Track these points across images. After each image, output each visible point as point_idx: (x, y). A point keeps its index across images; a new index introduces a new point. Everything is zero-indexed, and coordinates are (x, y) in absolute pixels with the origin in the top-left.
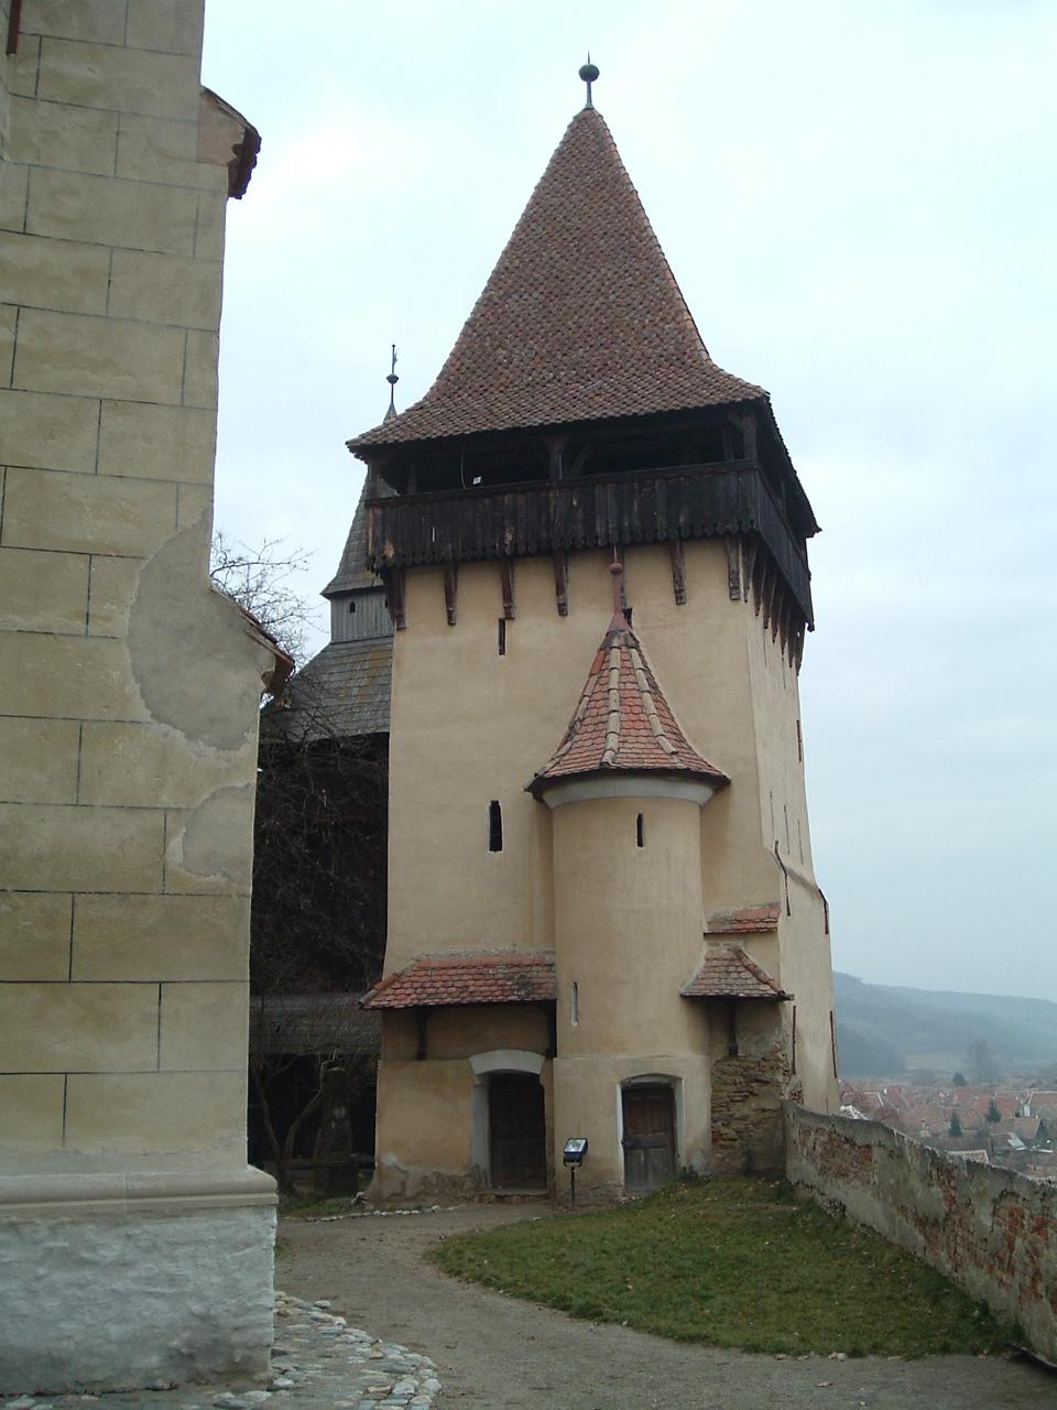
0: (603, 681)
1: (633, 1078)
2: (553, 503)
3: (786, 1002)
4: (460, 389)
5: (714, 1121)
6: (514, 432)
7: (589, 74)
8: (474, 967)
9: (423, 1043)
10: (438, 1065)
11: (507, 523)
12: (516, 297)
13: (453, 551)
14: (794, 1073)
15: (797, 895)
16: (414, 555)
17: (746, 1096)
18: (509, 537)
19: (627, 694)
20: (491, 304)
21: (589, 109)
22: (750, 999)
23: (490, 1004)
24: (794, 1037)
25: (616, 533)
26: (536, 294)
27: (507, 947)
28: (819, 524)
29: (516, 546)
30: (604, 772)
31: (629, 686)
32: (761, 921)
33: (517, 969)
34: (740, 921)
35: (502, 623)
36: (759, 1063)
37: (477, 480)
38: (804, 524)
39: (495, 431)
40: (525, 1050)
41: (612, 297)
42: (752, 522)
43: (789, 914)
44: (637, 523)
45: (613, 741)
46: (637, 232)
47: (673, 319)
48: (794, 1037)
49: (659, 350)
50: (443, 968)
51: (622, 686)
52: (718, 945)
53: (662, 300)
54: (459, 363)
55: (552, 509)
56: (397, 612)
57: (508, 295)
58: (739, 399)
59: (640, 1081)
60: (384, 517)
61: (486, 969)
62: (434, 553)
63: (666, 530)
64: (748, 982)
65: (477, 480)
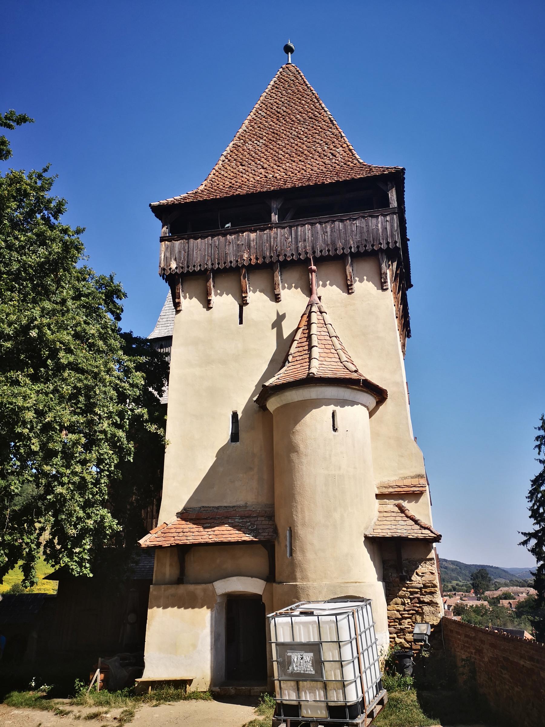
17: (413, 614)
18: (246, 256)
19: (322, 338)
22: (417, 539)
29: (250, 260)
31: (323, 333)
34: (399, 486)
36: (421, 589)
40: (252, 577)
45: (315, 363)
50: (198, 519)
51: (319, 333)
55: (272, 240)
56: (177, 300)
64: (413, 527)
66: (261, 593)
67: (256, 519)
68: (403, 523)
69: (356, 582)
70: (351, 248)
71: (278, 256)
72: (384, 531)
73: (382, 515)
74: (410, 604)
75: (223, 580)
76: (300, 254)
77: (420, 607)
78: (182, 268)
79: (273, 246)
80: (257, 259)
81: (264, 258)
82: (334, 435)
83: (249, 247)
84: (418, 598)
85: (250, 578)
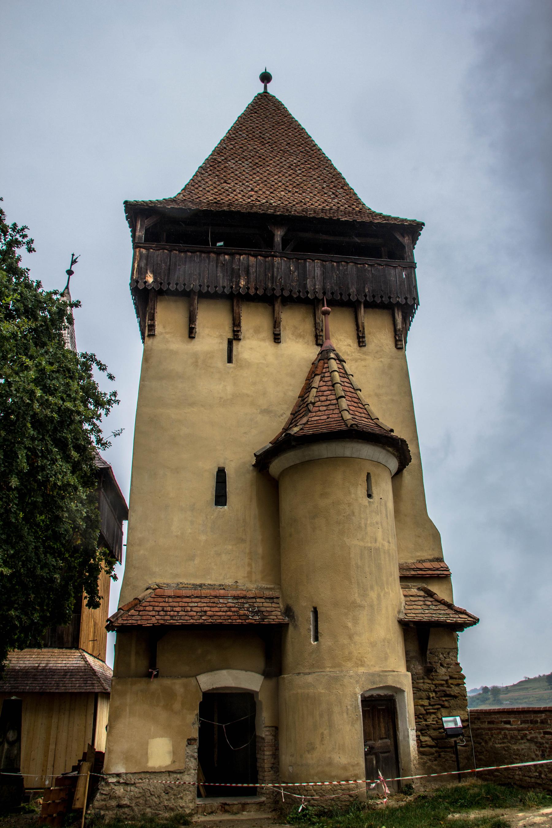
7: (266, 78)
8: (206, 597)
9: (153, 664)
10: (167, 682)
13: (200, 286)
17: (438, 709)
18: (242, 283)
21: (265, 92)
29: (248, 288)
35: (230, 343)
36: (446, 681)
40: (246, 671)
44: (336, 288)
50: (178, 597)
55: (275, 270)
62: (185, 285)
66: (257, 689)
68: (433, 607)
69: (394, 671)
70: (365, 296)
71: (282, 290)
73: (408, 599)
74: (435, 698)
75: (210, 673)
77: (446, 700)
78: (161, 284)
79: (277, 278)
80: (256, 289)
82: (369, 502)
83: (248, 273)
84: (444, 691)
85: (244, 672)
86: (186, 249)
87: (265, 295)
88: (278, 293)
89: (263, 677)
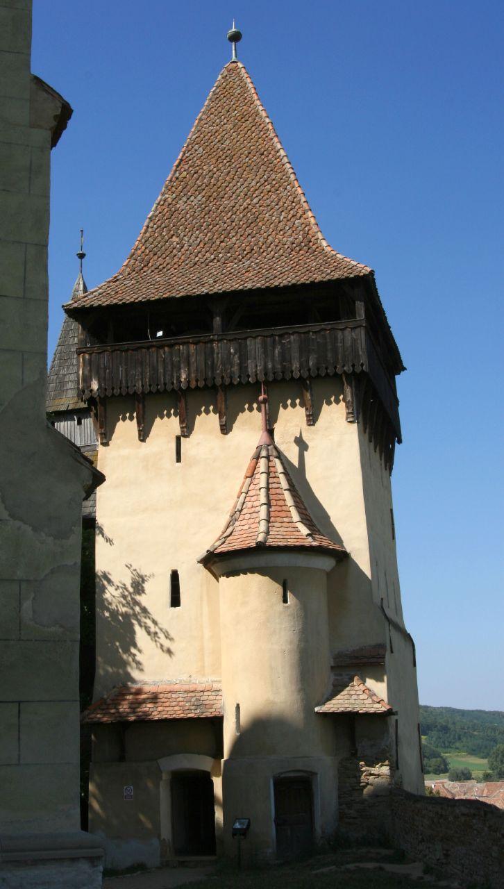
0: (255, 482)
1: (282, 773)
2: (216, 351)
3: (392, 717)
4: (145, 266)
5: (340, 804)
6: (187, 299)
11: (182, 366)
12: (185, 199)
13: (143, 386)
14: (398, 769)
15: (395, 636)
16: (113, 389)
18: (184, 376)
20: (166, 204)
22: (367, 714)
23: (175, 720)
24: (397, 742)
25: (263, 373)
26: (199, 197)
27: (185, 677)
28: (405, 365)
29: (189, 382)
30: (261, 548)
32: (373, 657)
33: (193, 694)
35: (178, 439)
37: (160, 334)
38: (394, 364)
39: (173, 298)
41: (255, 200)
42: (362, 365)
43: (392, 652)
46: (273, 152)
47: (301, 217)
48: (397, 742)
49: (291, 239)
52: (341, 675)
53: (293, 202)
54: (143, 248)
55: (215, 356)
57: (178, 198)
58: (352, 276)
59: (283, 775)
60: (90, 360)
61: (170, 694)
63: (300, 371)
64: (366, 702)
65: (160, 334)
67: (202, 694)
72: (335, 706)
76: (248, 376)
80: (197, 381)
81: (205, 380)
86: (126, 347)
87: (206, 385)
88: (218, 382)
89: (213, 760)
